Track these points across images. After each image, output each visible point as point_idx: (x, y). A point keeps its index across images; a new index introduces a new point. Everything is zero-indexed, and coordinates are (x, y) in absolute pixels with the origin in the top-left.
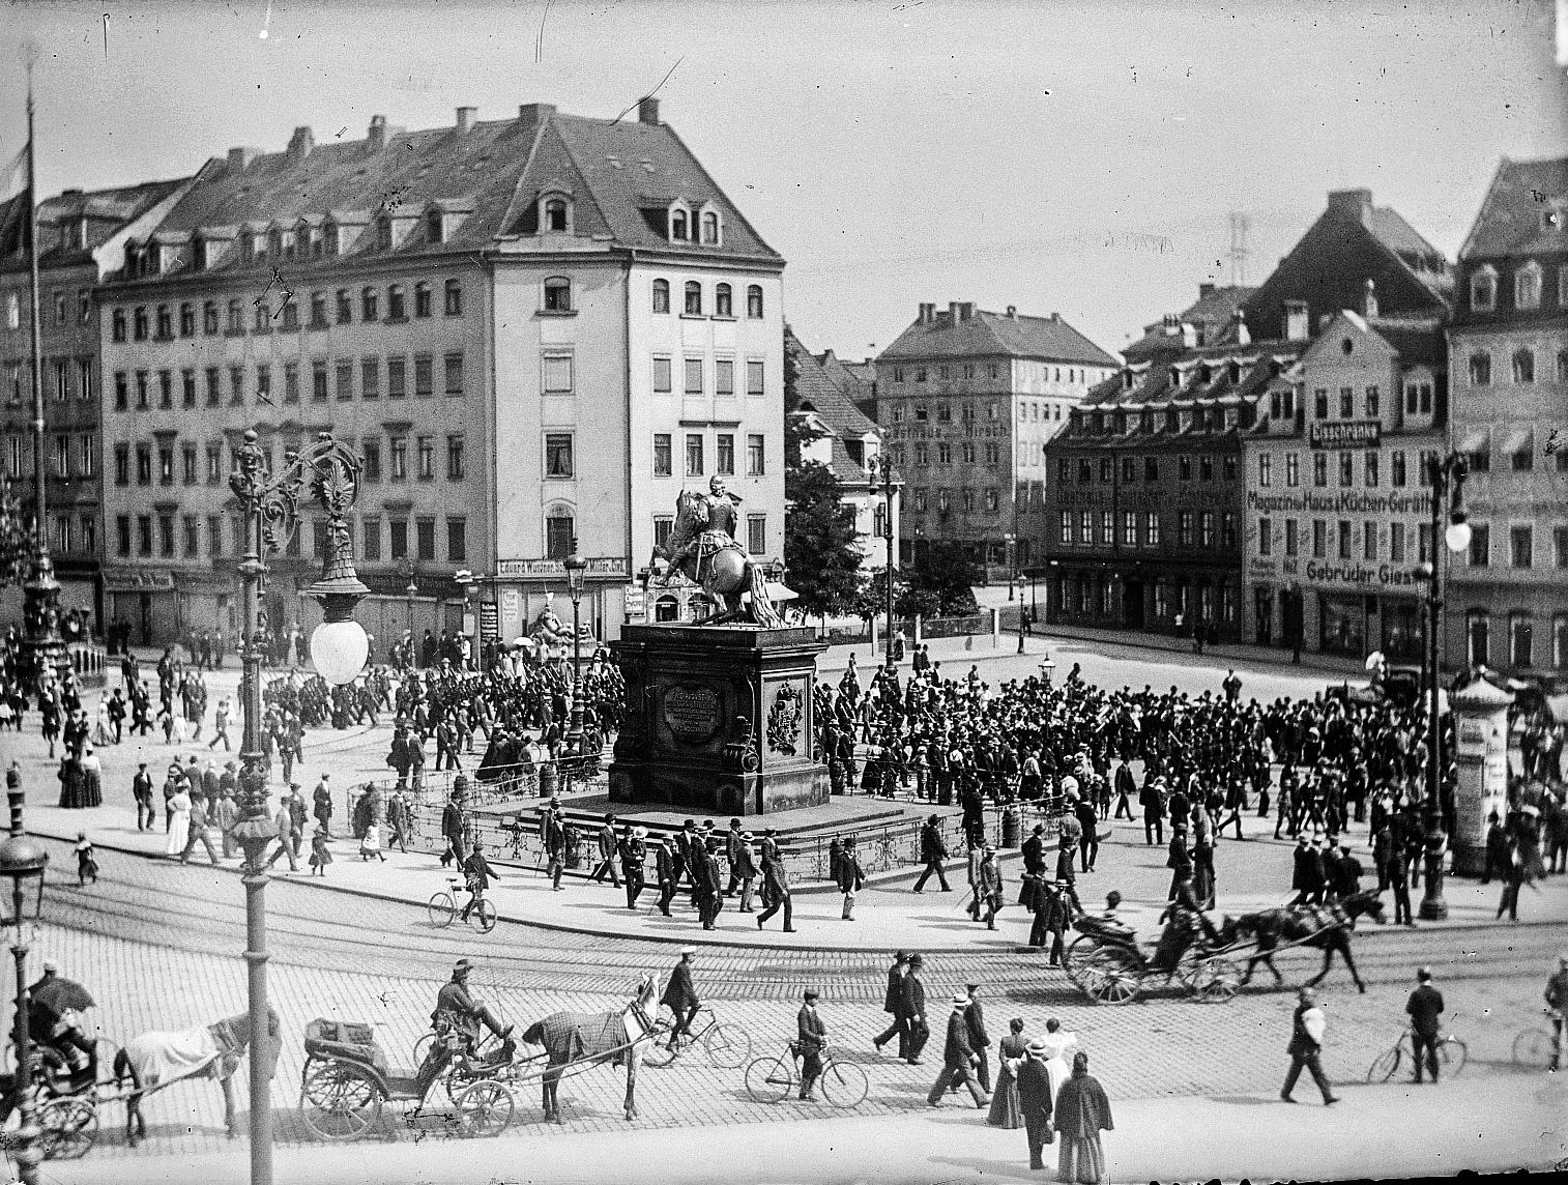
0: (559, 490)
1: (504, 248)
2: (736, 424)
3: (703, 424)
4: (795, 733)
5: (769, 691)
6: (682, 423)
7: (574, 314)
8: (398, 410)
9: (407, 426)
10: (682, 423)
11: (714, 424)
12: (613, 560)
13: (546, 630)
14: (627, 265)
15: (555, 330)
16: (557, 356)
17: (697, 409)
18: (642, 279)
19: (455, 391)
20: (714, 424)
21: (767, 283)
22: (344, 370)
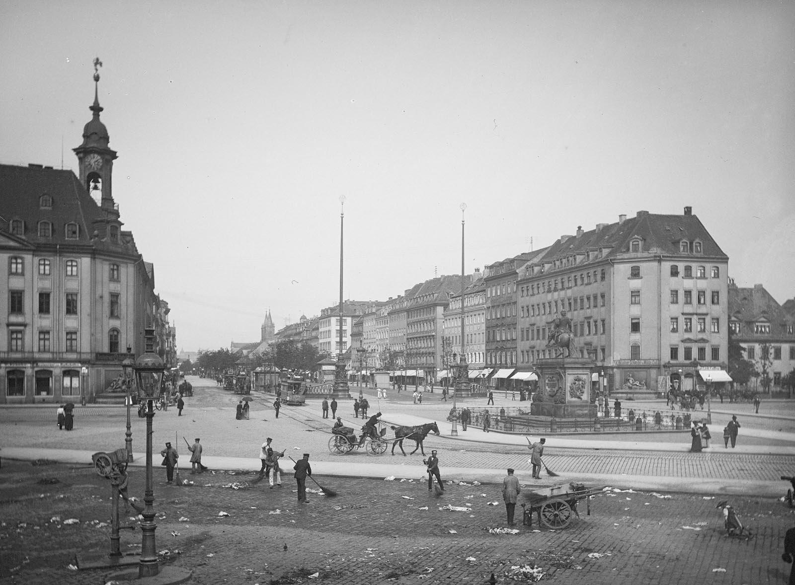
0: (636, 337)
1: (618, 257)
2: (707, 314)
3: (692, 314)
4: (583, 393)
5: (569, 379)
6: (683, 314)
7: (642, 278)
8: (588, 312)
9: (590, 318)
10: (683, 314)
11: (696, 314)
12: (653, 360)
13: (629, 384)
14: (660, 261)
15: (635, 284)
16: (635, 294)
17: (688, 309)
18: (667, 266)
19: (603, 306)
20: (696, 314)
21: (721, 266)
22: (575, 300)
